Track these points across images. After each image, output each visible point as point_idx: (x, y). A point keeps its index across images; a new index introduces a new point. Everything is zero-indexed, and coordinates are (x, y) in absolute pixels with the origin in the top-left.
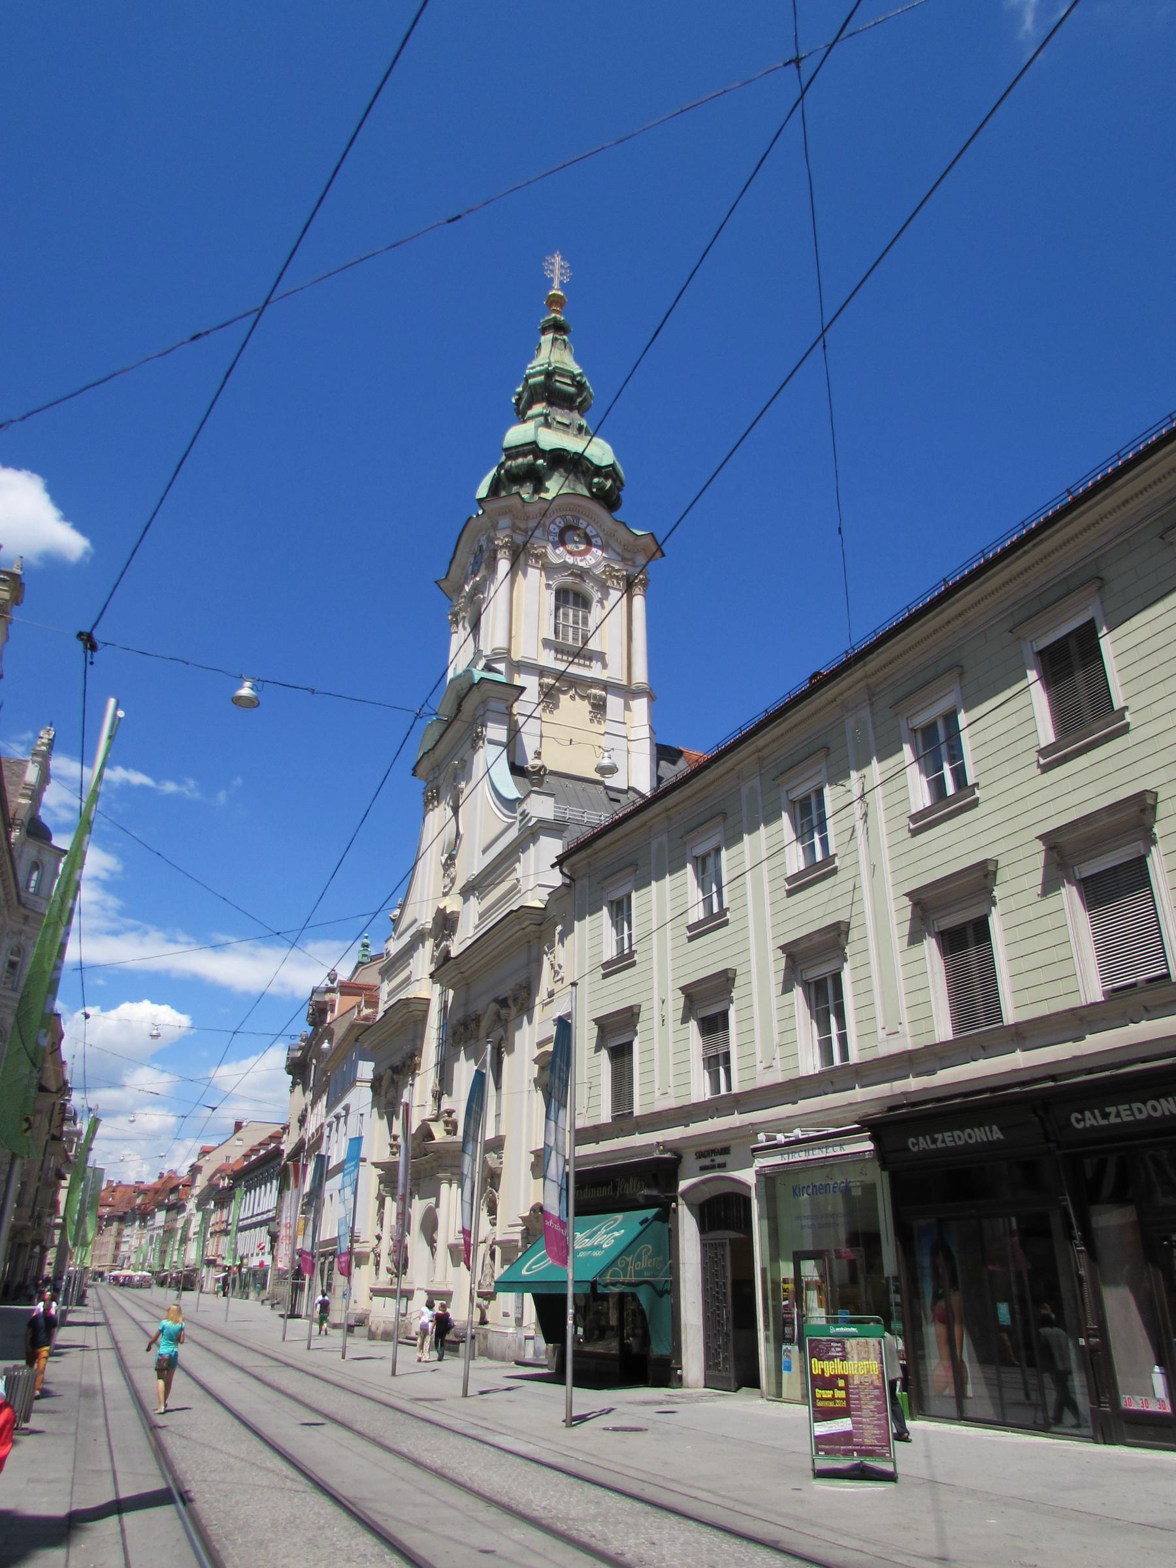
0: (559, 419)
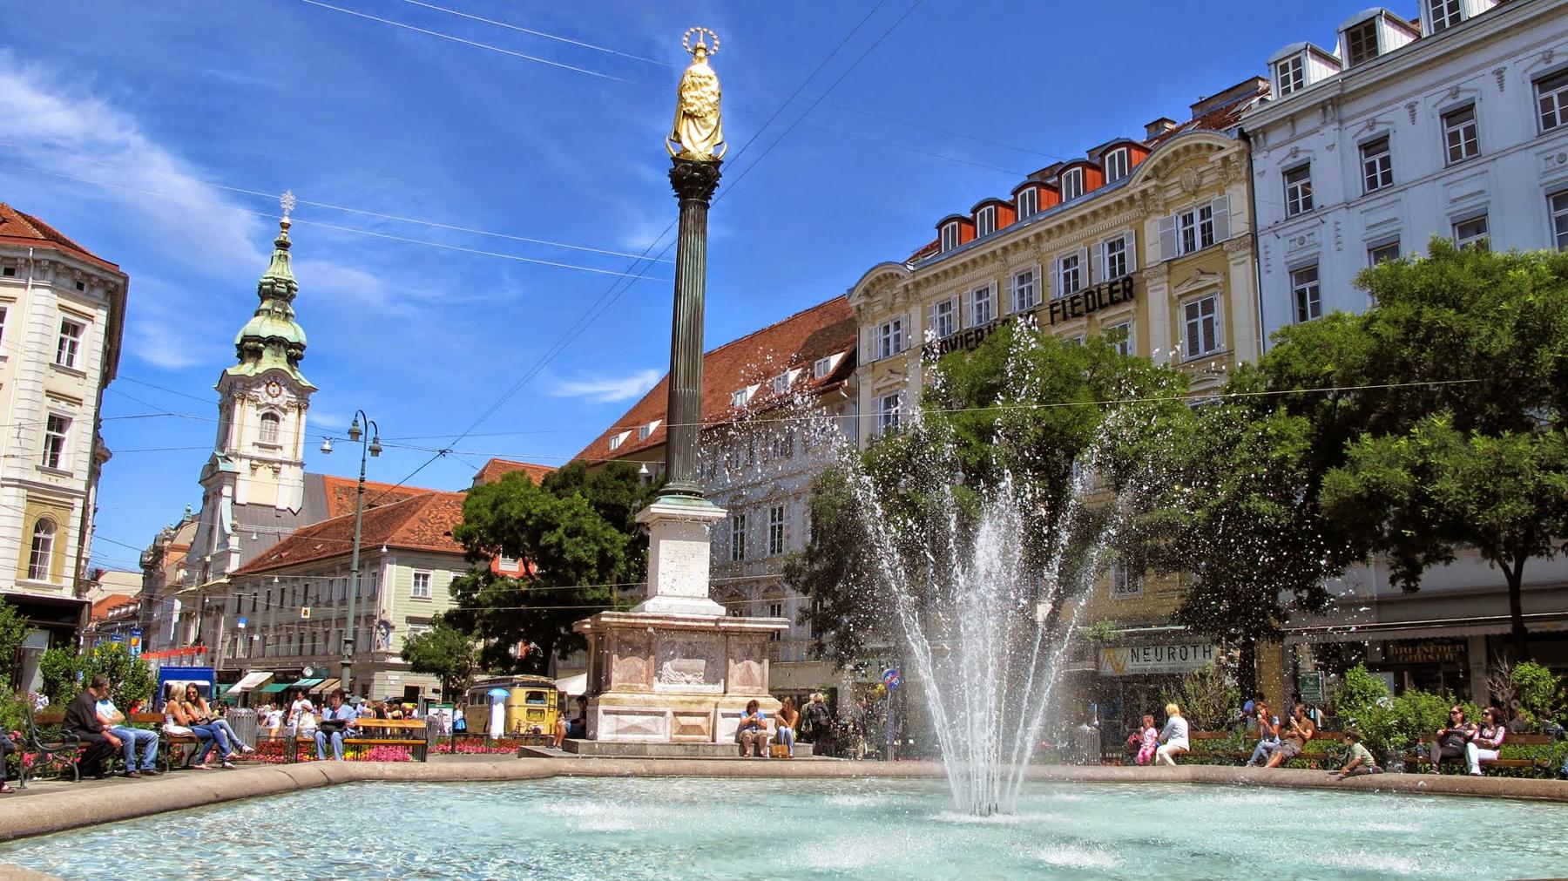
0: (276, 309)
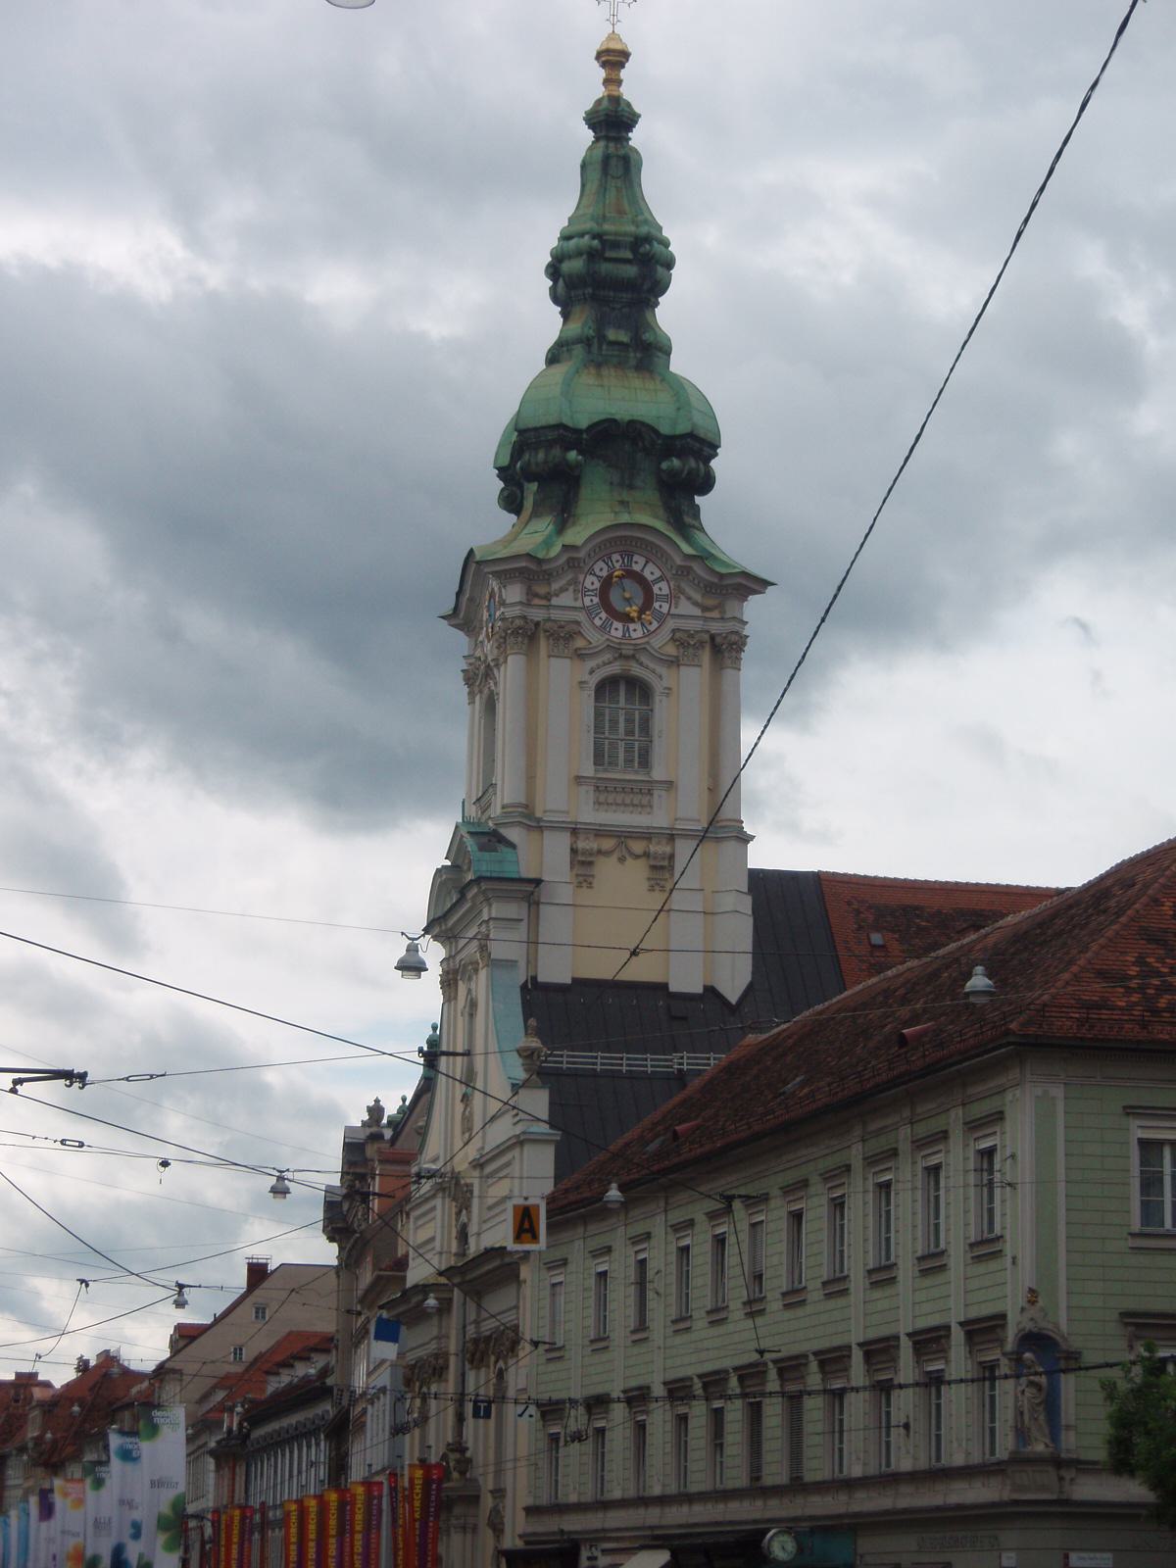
0: (612, 334)
